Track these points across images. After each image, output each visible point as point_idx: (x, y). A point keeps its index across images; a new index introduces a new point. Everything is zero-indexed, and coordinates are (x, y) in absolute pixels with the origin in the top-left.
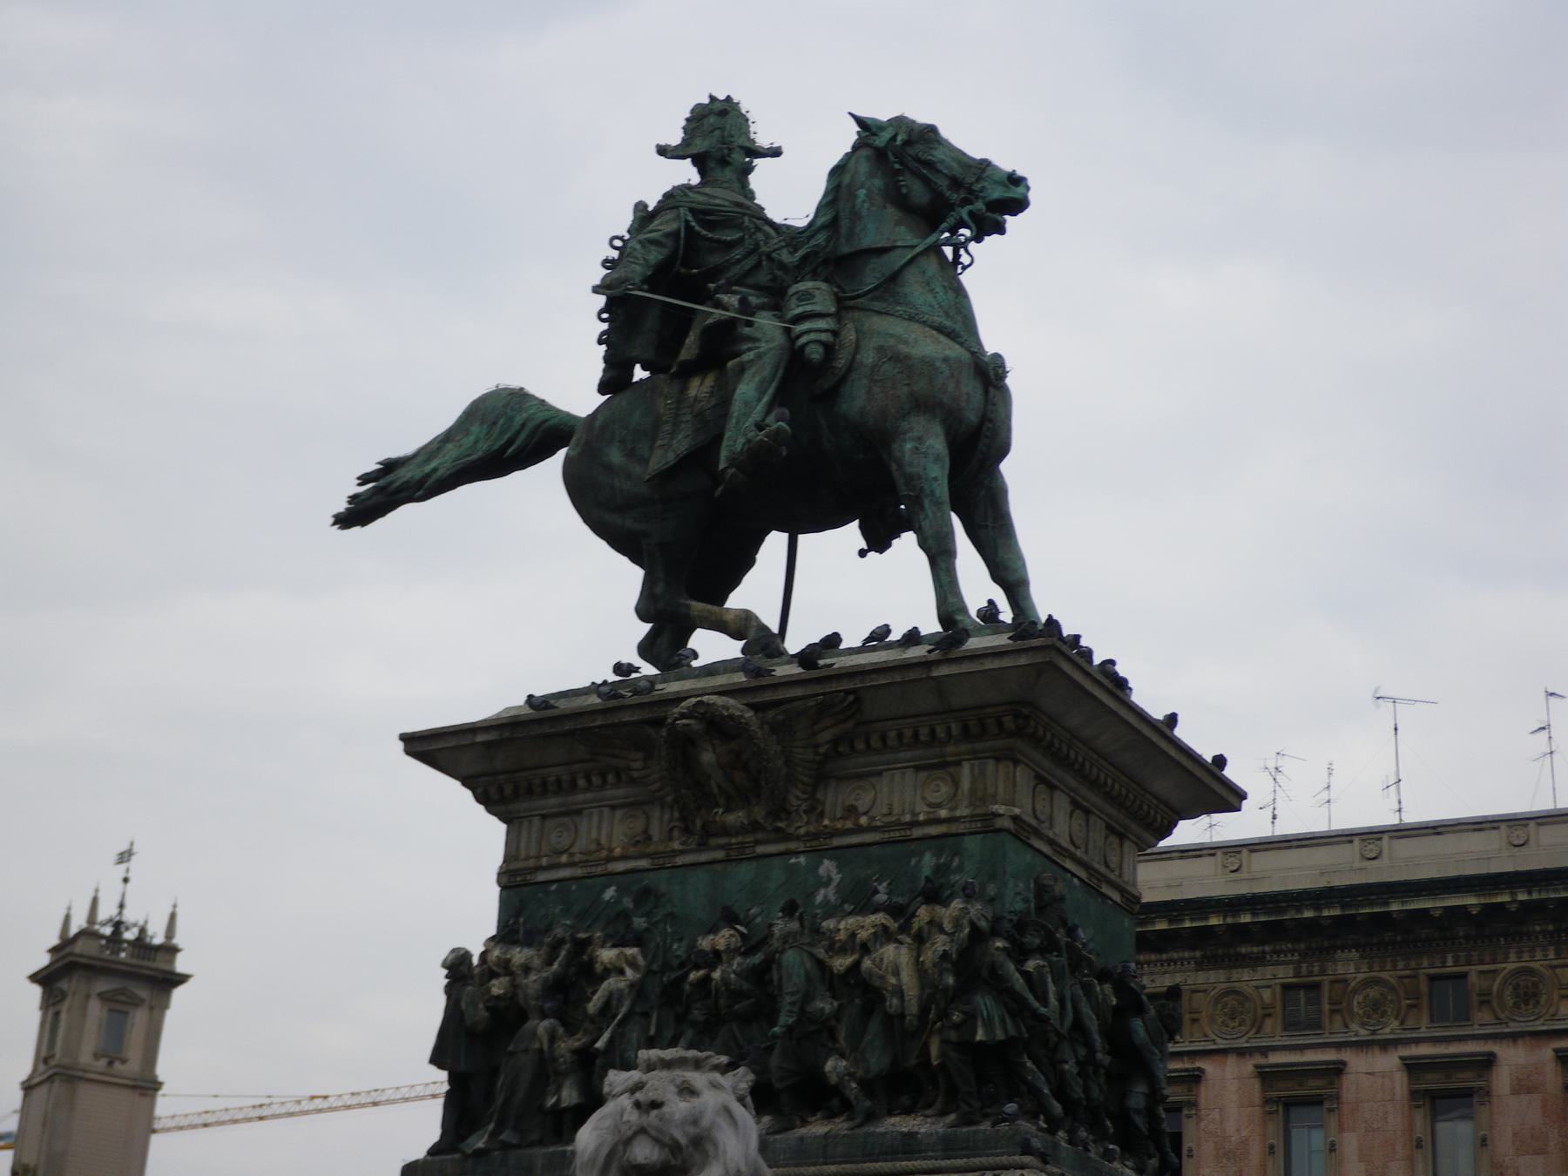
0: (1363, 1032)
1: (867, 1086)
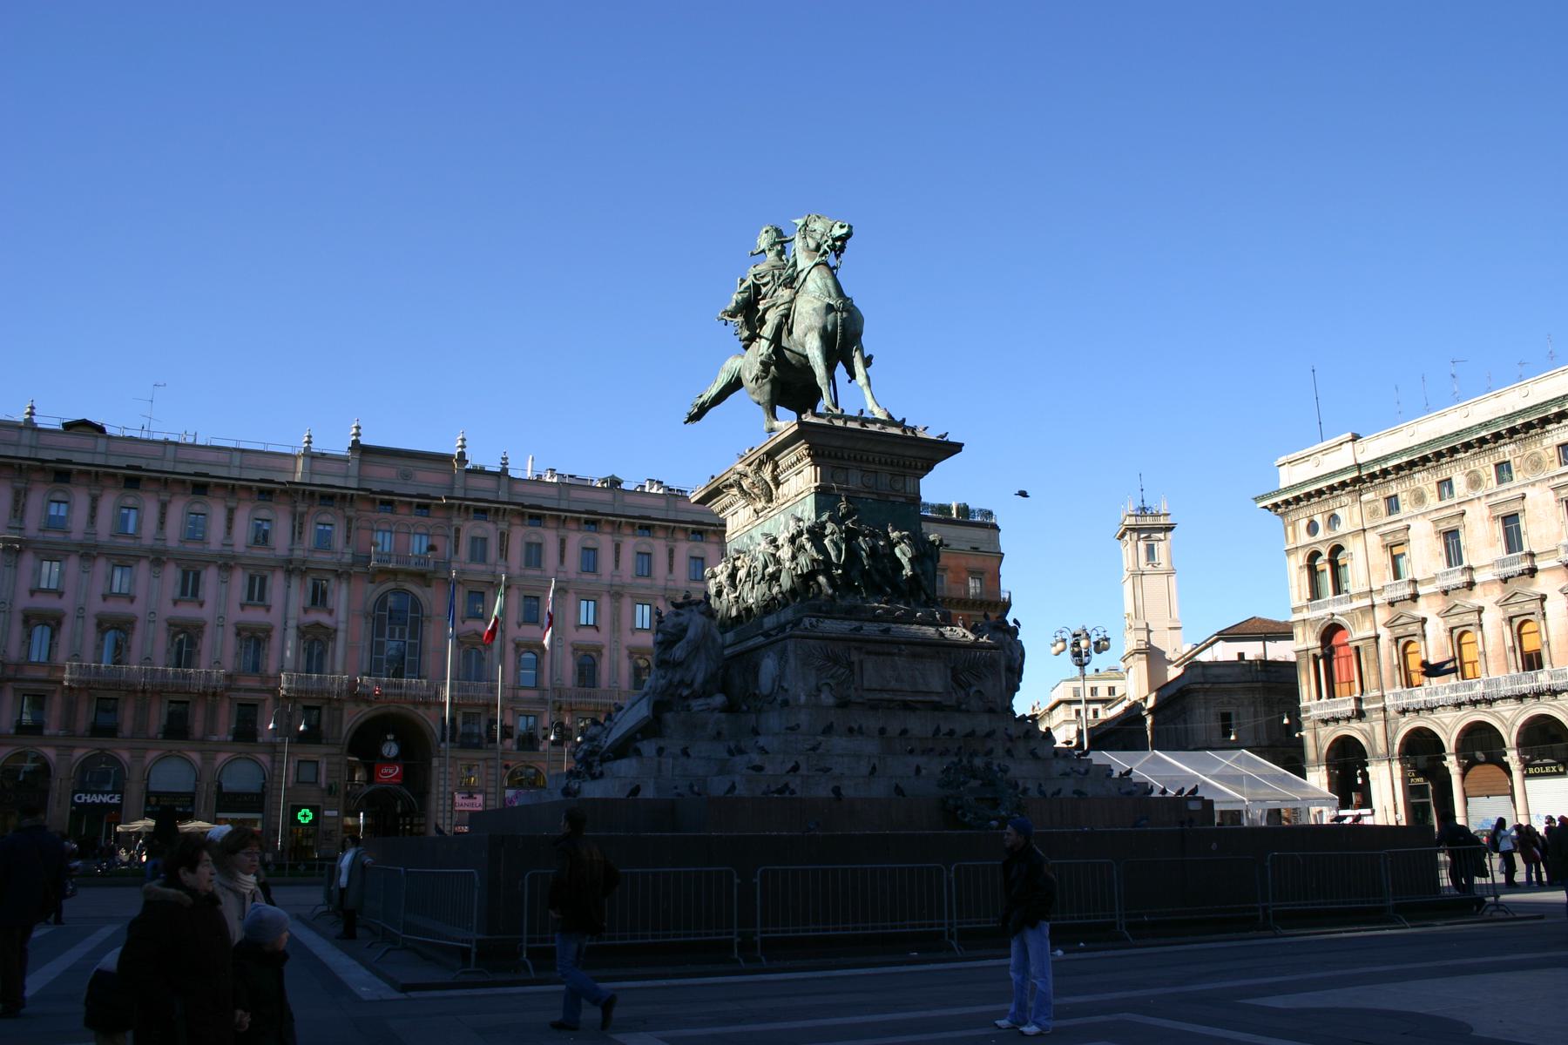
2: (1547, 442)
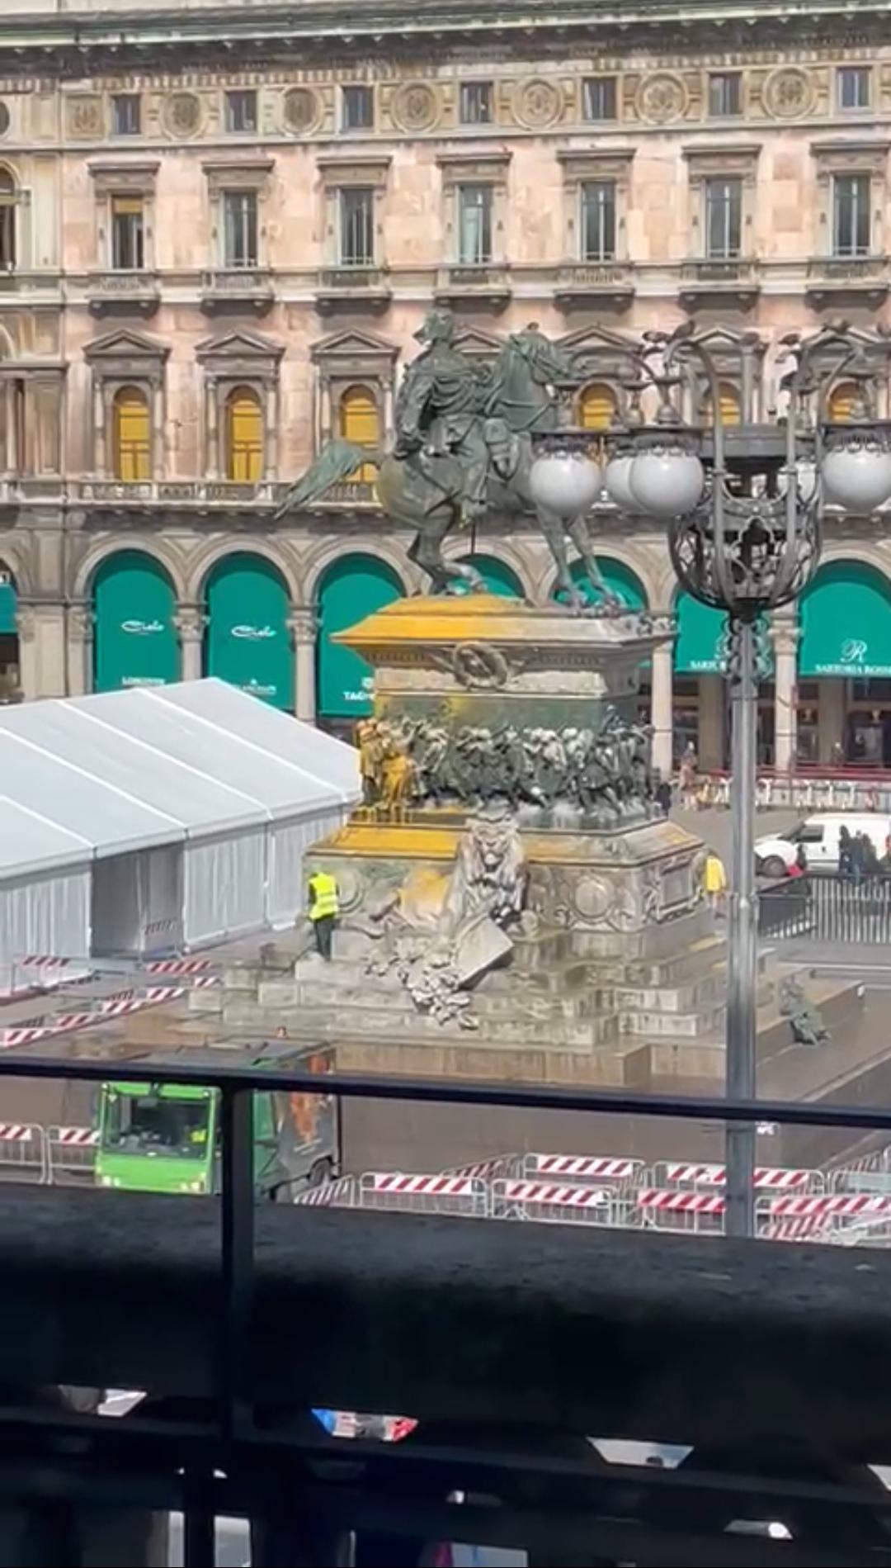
0: (651, 122)
1: (547, 797)
2: (446, 71)
